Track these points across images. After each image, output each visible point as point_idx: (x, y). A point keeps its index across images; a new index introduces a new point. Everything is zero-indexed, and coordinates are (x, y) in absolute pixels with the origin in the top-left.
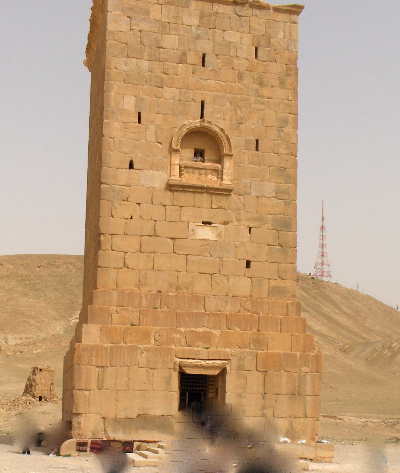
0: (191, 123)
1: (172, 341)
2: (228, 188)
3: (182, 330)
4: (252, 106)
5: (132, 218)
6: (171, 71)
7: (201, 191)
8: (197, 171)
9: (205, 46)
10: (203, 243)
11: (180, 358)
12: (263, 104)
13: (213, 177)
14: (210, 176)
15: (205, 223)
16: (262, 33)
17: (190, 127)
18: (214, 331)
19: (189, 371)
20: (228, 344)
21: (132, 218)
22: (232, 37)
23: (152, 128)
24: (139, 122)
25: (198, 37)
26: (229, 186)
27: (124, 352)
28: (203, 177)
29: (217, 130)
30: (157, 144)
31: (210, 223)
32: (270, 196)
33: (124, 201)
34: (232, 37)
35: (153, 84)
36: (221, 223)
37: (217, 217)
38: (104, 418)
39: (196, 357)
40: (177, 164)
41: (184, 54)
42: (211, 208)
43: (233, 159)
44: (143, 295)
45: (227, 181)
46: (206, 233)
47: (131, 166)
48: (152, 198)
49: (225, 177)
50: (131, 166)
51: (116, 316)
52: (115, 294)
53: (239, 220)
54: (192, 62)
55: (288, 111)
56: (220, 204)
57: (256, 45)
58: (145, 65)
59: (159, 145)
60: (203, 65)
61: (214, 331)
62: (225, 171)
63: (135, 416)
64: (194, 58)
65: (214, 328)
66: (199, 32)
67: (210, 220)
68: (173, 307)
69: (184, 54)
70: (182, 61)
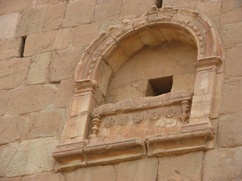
0: (126, 24)
2: (196, 133)
7: (130, 156)
8: (131, 116)
13: (168, 121)
14: (160, 123)
17: (124, 32)
23: (43, 59)
26: (197, 128)
28: (144, 127)
30: (50, 85)
40: (83, 114)
43: (222, 70)
45: (200, 118)
49: (193, 112)
59: (54, 86)
62: (195, 99)
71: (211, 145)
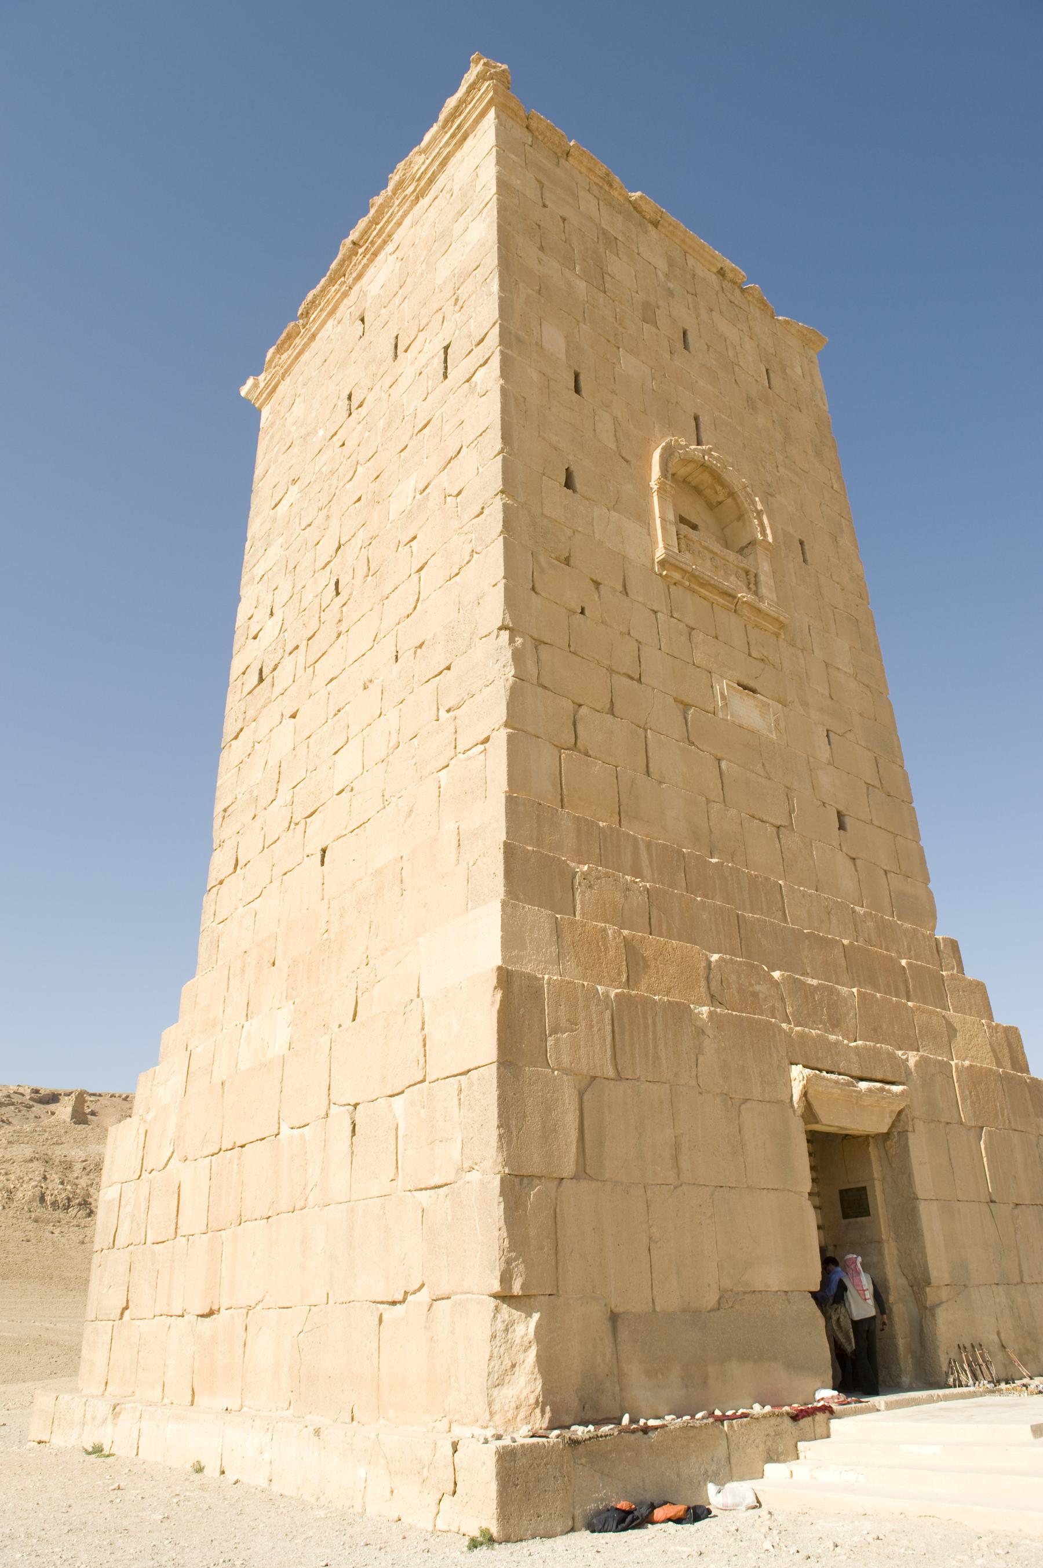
4: (781, 469)
5: (582, 612)
21: (582, 612)
27: (654, 1023)
33: (557, 559)
38: (614, 1318)
42: (750, 655)
44: (641, 843)
46: (747, 712)
47: (569, 484)
48: (624, 580)
50: (569, 484)
53: (805, 704)
56: (765, 654)
58: (581, 286)
62: (762, 578)
63: (711, 1299)
67: (752, 684)
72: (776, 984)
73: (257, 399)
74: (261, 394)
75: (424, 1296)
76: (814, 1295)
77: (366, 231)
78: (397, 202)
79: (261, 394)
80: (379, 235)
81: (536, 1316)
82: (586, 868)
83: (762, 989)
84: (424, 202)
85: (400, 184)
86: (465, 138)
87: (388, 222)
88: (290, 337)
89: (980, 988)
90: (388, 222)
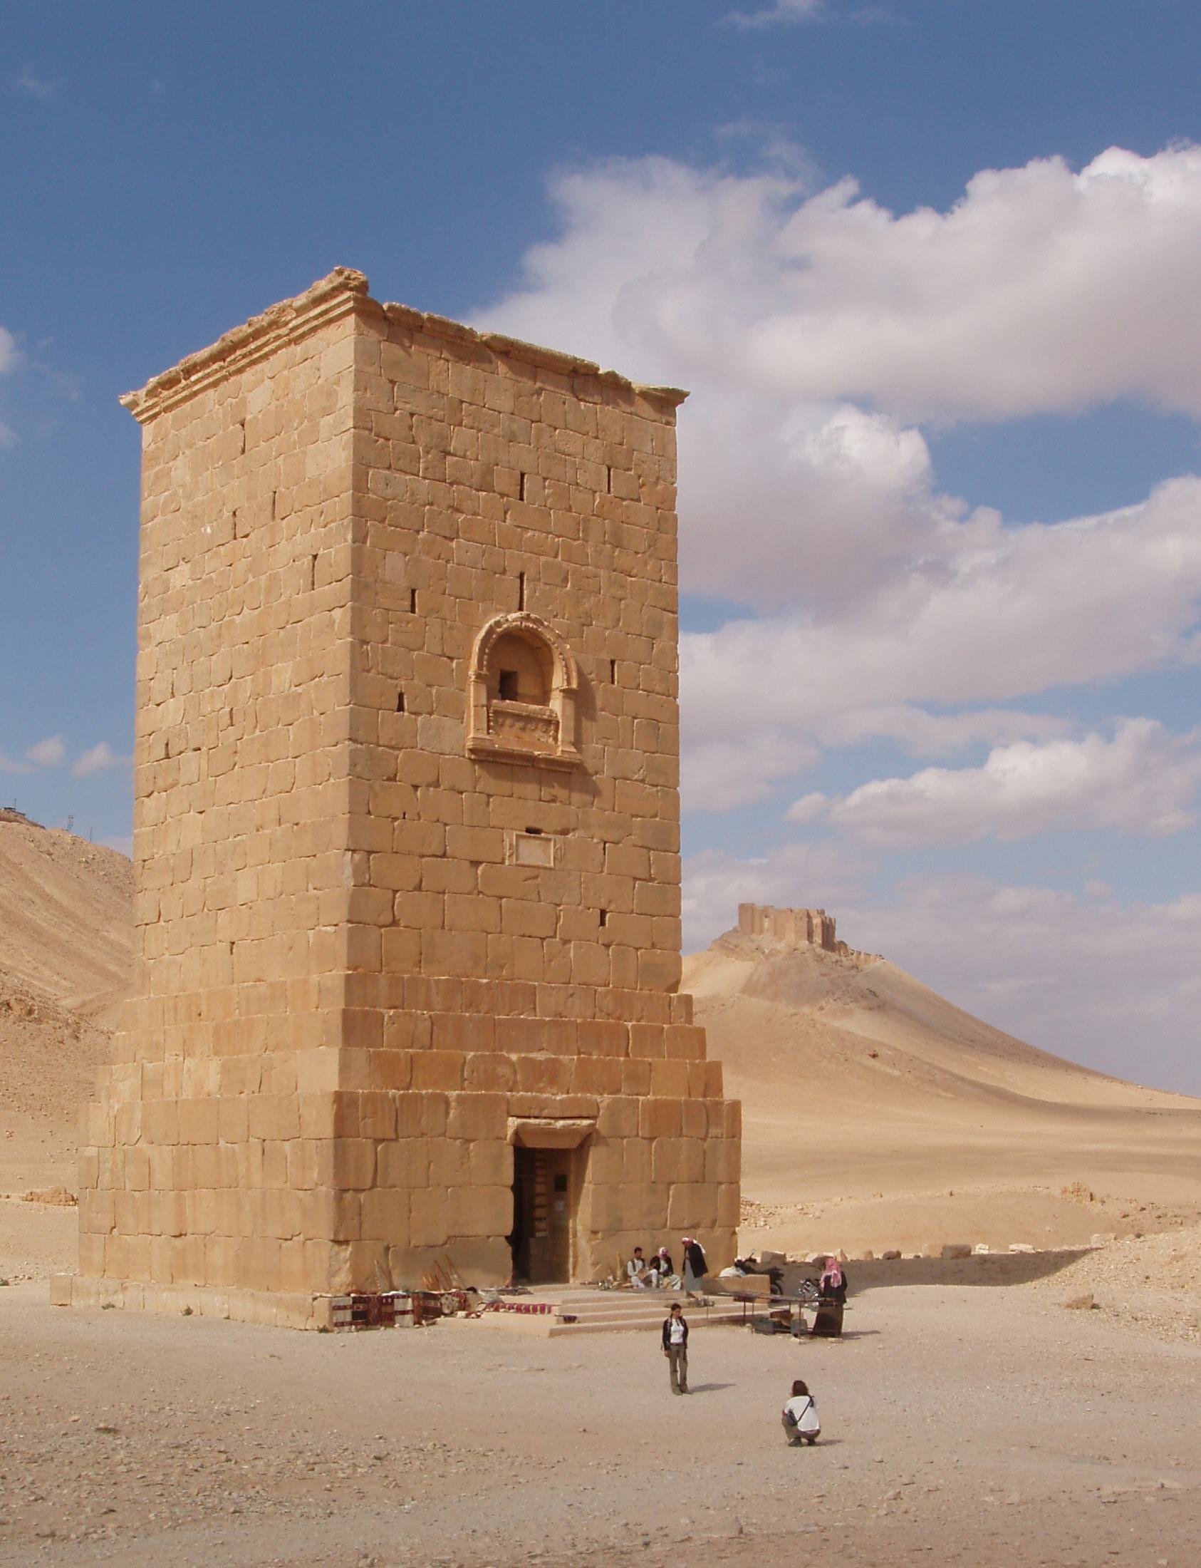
1: (491, 1081)
3: (514, 1057)
6: (467, 505)
9: (522, 455)
10: (530, 873)
11: (518, 1117)
12: (623, 587)
15: (529, 830)
16: (618, 440)
18: (564, 1058)
19: (530, 1143)
20: (585, 1085)
22: (570, 442)
24: (413, 612)
25: (512, 438)
29: (548, 636)
31: (537, 831)
32: (636, 777)
34: (570, 442)
35: (437, 531)
36: (556, 832)
37: (551, 817)
39: (545, 1113)
41: (488, 471)
46: (533, 853)
51: (389, 1030)
52: (383, 979)
54: (505, 490)
55: (662, 604)
57: (608, 462)
60: (522, 499)
61: (564, 1058)
64: (502, 480)
65: (558, 1051)
66: (515, 427)
67: (538, 826)
68: (484, 1007)
69: (488, 471)
70: (485, 486)
71: (575, 770)
72: (511, 1064)
73: (138, 414)
74: (142, 412)
75: (301, 1238)
76: (507, 1238)
77: (243, 342)
78: (273, 334)
79: (142, 412)
80: (258, 349)
81: (350, 1249)
82: (392, 1012)
83: (503, 1070)
84: (298, 349)
85: (274, 324)
86: (331, 321)
87: (265, 345)
88: (170, 383)
89: (701, 1033)
90: (265, 345)
